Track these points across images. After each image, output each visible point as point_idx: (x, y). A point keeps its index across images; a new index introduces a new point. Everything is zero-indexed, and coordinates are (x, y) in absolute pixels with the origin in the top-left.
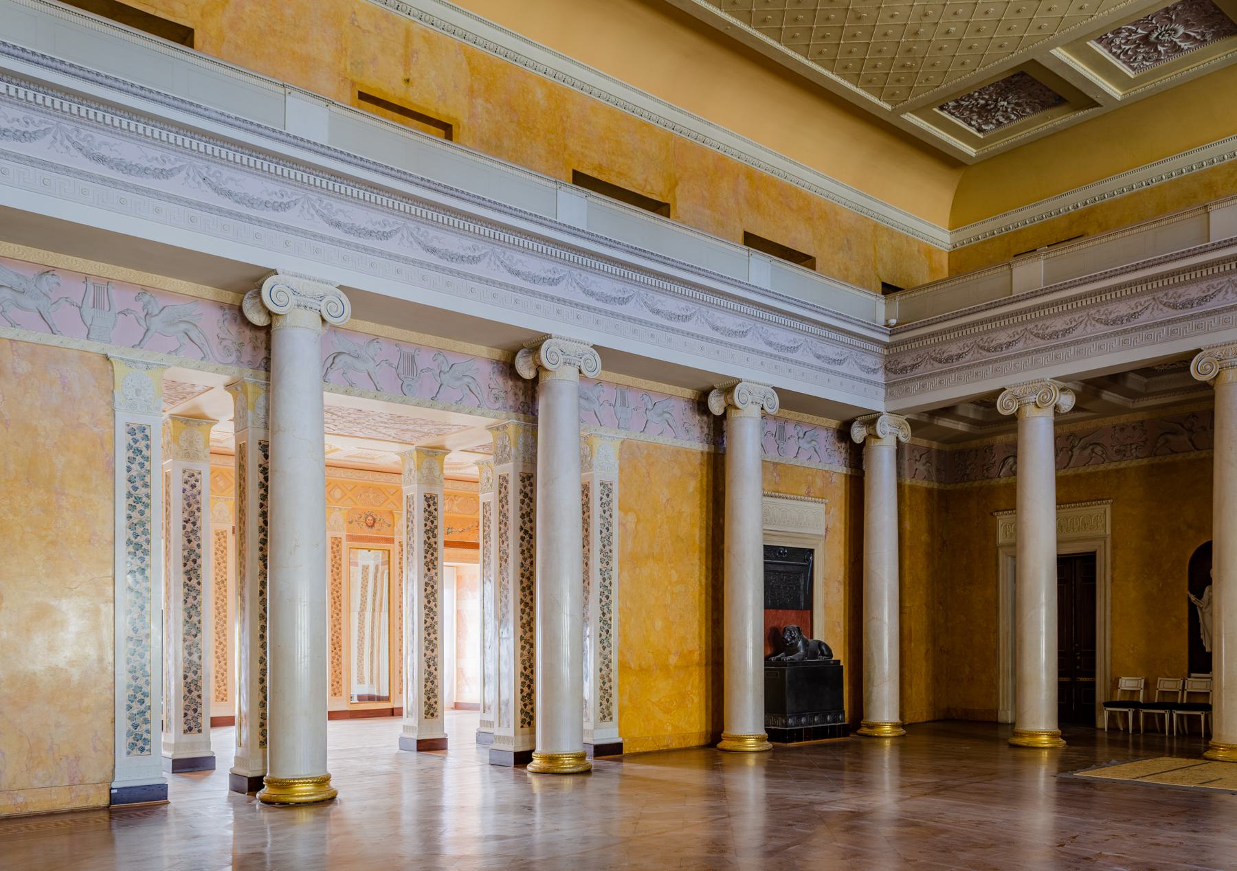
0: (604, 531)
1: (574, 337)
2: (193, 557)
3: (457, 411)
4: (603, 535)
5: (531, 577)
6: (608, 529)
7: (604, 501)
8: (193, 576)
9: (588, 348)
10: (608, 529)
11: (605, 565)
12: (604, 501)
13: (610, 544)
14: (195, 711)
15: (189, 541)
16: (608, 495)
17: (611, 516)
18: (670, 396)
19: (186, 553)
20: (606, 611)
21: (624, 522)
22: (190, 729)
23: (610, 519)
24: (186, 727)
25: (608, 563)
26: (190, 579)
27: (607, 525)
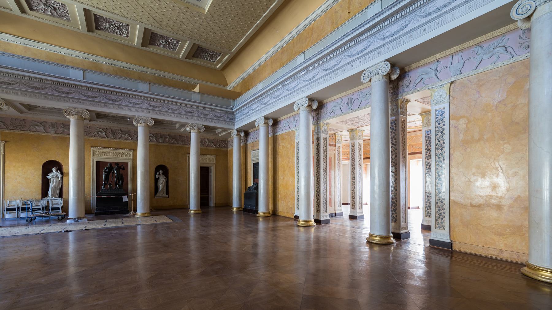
0: (439, 134)
1: (374, 64)
2: (354, 165)
3: (352, 112)
4: (438, 136)
5: (396, 162)
6: (442, 132)
7: (438, 119)
8: (354, 169)
9: (384, 63)
10: (442, 132)
11: (440, 150)
12: (438, 119)
13: (443, 139)
14: (354, 204)
15: (353, 161)
16: (442, 115)
17: (444, 125)
18: (505, 34)
19: (352, 164)
20: (318, 178)
21: (456, 125)
22: (353, 208)
23: (443, 127)
24: (352, 207)
25: (442, 150)
26: (353, 170)
27: (441, 130)
